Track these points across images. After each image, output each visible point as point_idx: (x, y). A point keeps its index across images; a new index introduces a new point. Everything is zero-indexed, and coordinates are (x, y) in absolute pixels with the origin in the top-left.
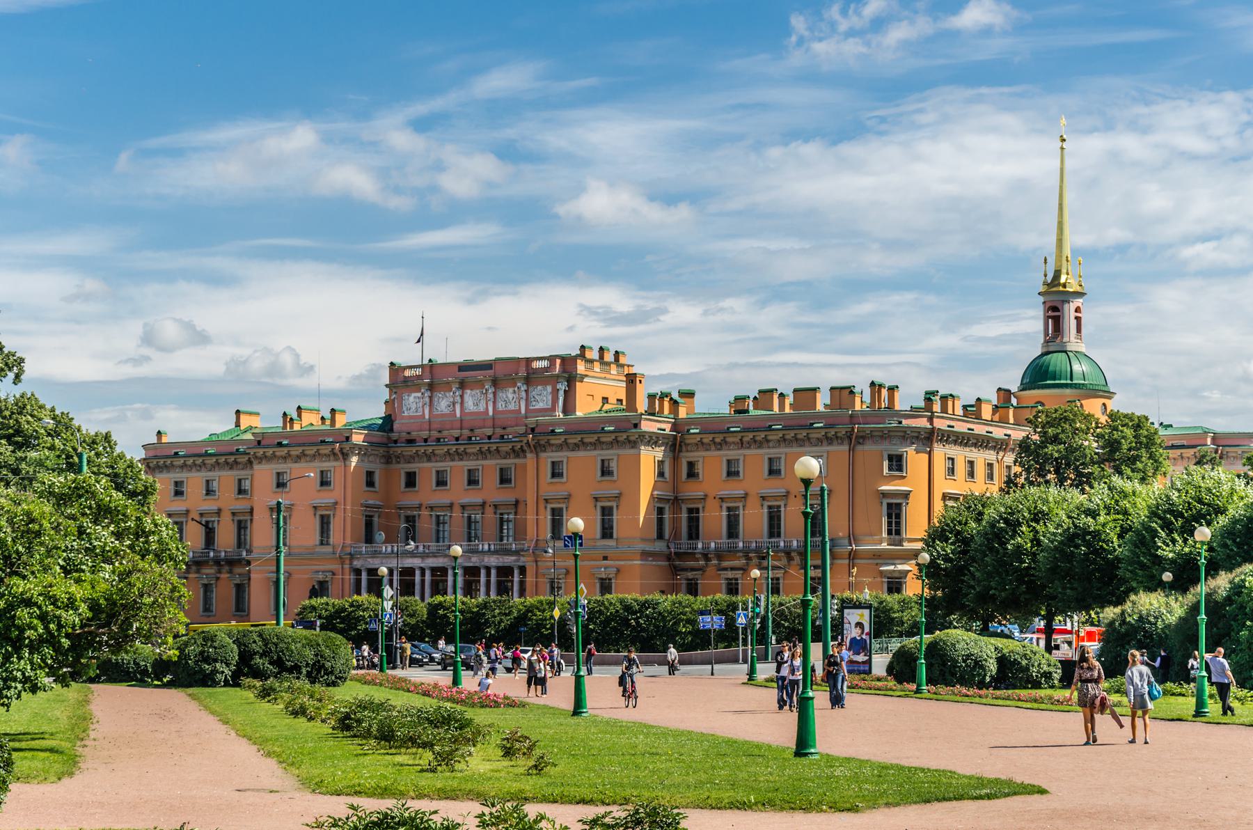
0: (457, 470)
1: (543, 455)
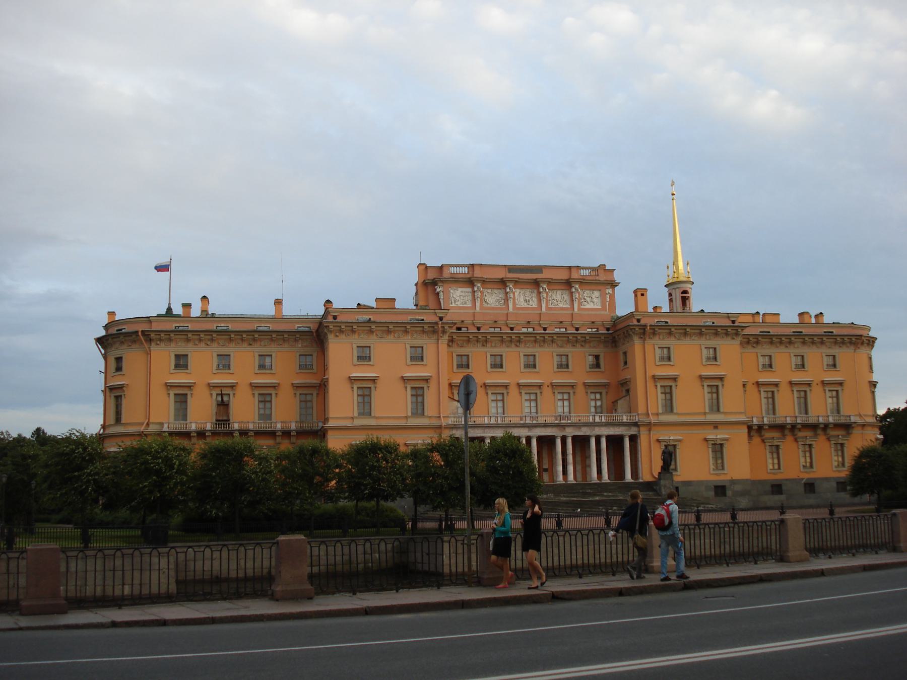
0: (514, 357)
1: (652, 342)
